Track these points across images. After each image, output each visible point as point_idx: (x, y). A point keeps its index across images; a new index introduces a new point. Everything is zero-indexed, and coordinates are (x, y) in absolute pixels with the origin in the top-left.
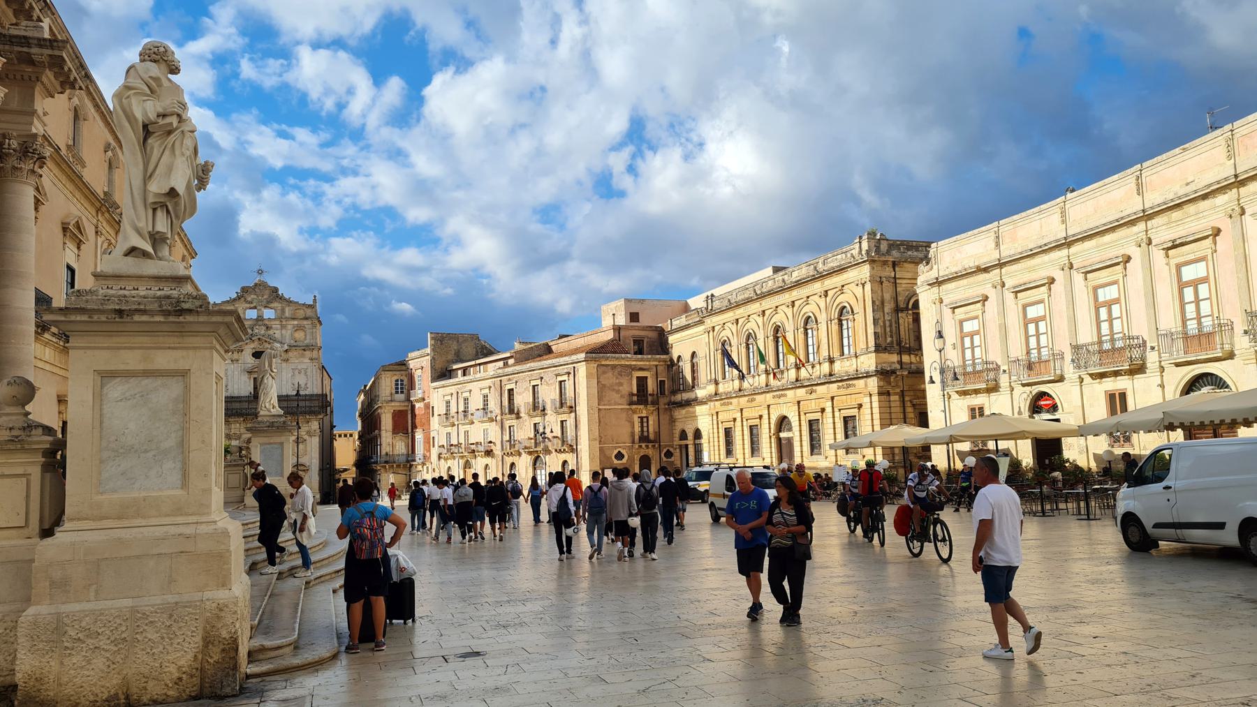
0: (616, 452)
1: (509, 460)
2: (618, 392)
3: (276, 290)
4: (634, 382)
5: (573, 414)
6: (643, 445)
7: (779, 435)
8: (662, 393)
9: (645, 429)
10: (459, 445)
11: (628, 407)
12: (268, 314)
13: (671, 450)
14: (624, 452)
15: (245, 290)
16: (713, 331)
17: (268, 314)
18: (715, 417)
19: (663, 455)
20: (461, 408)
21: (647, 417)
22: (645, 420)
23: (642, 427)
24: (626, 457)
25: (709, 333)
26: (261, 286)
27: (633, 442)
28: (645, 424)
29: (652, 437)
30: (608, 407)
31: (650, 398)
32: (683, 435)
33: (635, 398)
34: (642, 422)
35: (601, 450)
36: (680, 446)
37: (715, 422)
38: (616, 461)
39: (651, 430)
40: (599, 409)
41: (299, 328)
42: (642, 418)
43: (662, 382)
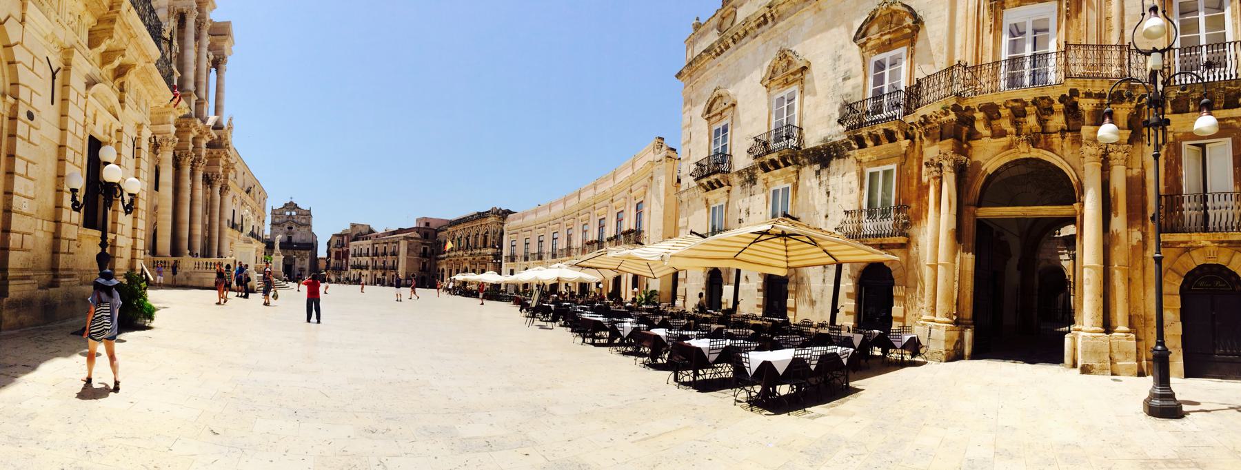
1: (374, 272)
2: (415, 252)
3: (296, 205)
8: (433, 254)
12: (294, 213)
15: (286, 204)
17: (294, 213)
26: (291, 203)
27: (420, 271)
31: (428, 255)
35: (406, 272)
41: (304, 218)
43: (433, 250)
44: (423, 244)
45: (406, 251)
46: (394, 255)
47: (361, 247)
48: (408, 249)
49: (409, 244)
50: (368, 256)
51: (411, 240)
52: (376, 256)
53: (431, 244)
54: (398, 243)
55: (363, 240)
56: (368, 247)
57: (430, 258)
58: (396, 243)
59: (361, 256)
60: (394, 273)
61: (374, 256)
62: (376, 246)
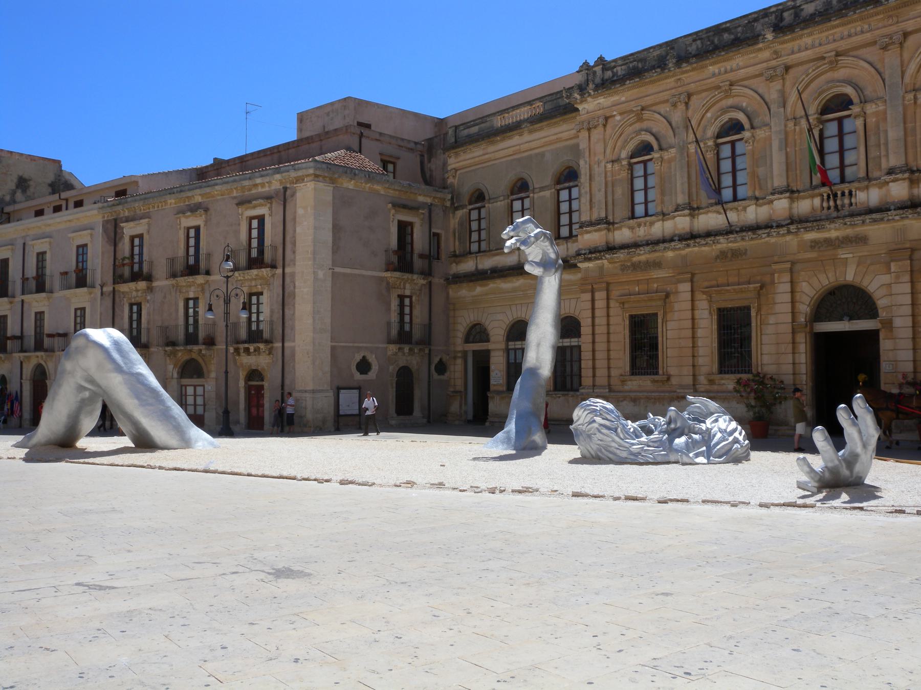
0: (358, 358)
4: (394, 230)
5: (278, 282)
6: (406, 348)
7: (812, 328)
9: (407, 319)
10: (21, 338)
11: (388, 274)
13: (445, 358)
14: (372, 359)
16: (605, 126)
18: (600, 296)
19: (433, 367)
20: (31, 272)
21: (410, 297)
22: (407, 301)
23: (402, 314)
24: (375, 367)
25: (589, 130)
28: (407, 310)
29: (417, 334)
30: (348, 271)
31: (418, 263)
32: (478, 333)
33: (395, 259)
34: (402, 306)
36: (465, 353)
37: (600, 304)
38: (358, 376)
39: (416, 320)
40: (333, 273)
42: (401, 298)
44: (400, 206)
45: (328, 236)
46: (256, 262)
47: (41, 246)
48: (337, 229)
49: (342, 202)
50: (81, 281)
51: (351, 185)
52: (136, 277)
53: (430, 207)
54: (284, 197)
55: (39, 213)
56: (83, 238)
57: (427, 273)
58: (268, 198)
59: (41, 287)
60: (261, 360)
61: (118, 279)
62: (129, 229)
